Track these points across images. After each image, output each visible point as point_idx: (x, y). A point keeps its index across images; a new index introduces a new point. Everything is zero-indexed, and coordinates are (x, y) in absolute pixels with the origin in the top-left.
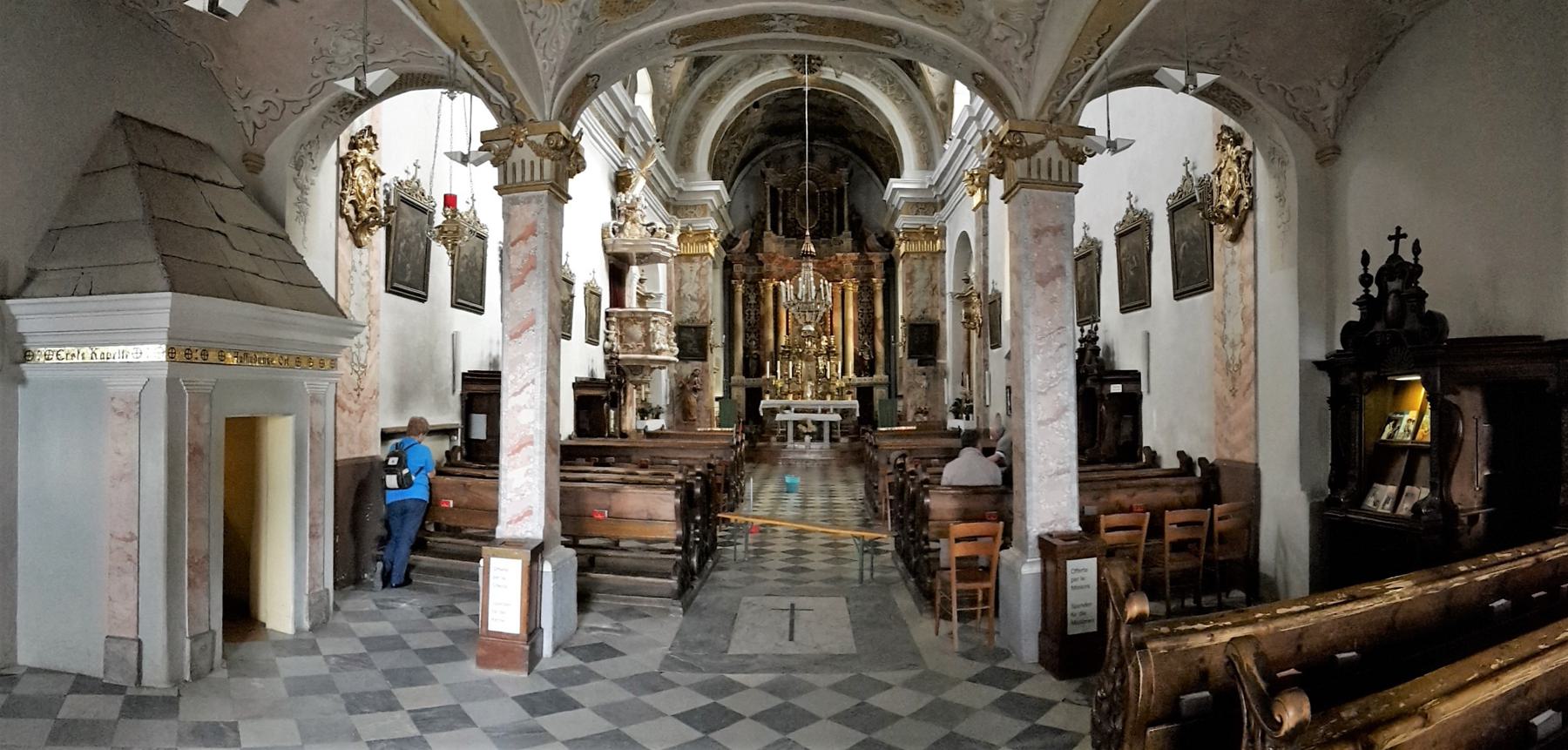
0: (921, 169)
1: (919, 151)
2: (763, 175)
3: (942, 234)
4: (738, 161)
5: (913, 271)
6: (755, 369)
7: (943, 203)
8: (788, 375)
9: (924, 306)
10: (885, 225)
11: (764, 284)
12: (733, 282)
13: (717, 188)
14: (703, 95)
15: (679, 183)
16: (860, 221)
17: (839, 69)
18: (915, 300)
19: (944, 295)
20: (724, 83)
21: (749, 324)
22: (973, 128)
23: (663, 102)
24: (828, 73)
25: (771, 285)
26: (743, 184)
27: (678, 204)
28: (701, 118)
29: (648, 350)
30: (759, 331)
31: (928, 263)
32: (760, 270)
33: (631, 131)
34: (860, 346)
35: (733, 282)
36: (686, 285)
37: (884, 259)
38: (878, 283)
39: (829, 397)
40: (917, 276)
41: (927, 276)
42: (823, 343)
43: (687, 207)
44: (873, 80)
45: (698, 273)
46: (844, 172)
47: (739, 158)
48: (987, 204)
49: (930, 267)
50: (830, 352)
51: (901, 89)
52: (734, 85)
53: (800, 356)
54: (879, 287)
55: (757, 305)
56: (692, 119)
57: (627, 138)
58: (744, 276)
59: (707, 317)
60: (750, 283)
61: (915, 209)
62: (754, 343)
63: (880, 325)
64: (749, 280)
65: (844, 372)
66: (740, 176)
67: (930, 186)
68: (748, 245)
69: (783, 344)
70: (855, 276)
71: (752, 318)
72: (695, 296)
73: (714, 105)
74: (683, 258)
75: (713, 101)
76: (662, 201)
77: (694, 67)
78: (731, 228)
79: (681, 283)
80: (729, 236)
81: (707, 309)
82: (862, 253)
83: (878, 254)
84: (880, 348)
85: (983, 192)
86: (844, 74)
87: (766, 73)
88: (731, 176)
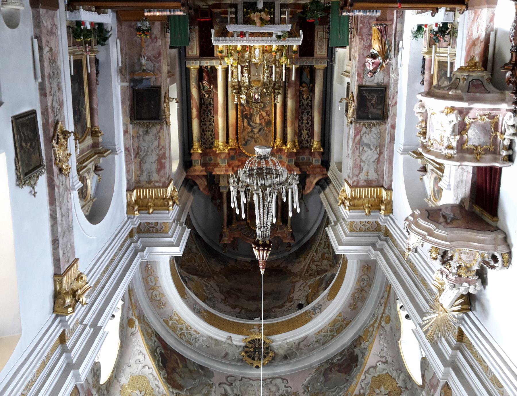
0: (155, 263)
1: (156, 278)
2: (292, 236)
3: (130, 206)
4: (314, 248)
5: (159, 171)
6: (305, 74)
7: (131, 234)
8: (276, 67)
9: (147, 138)
10: (192, 197)
11: (295, 146)
12: (322, 150)
13: (341, 248)
14: (347, 324)
15: (373, 254)
16: (213, 199)
17: (228, 344)
18: (156, 143)
19: (127, 149)
20: (329, 333)
21: (308, 113)
22: (75, 354)
23: (388, 328)
24: (238, 340)
25: (288, 146)
26: (309, 227)
27: (376, 233)
28: (350, 305)
29: (463, 113)
30: (300, 106)
31: (144, 178)
32: (297, 159)
33: (450, 351)
34: (212, 93)
35: (322, 150)
36: (372, 160)
37: (192, 169)
38: (196, 148)
39: (239, 48)
40: (155, 166)
41: (145, 166)
42: (244, 97)
43: (368, 230)
44: (198, 336)
45: (361, 170)
46: (226, 240)
47: (312, 254)
48: (55, 275)
49: (142, 174)
50: (239, 89)
51: (174, 329)
52: (321, 331)
53: (264, 84)
54: (196, 145)
55: (300, 129)
56: (359, 304)
57: (454, 342)
58: (311, 154)
59: (356, 129)
60: (307, 147)
61: (158, 227)
62: (305, 97)
63: (194, 112)
64: (307, 151)
65: (226, 71)
66: (311, 234)
67: (143, 250)
68: (308, 180)
69: (279, 96)
70: (216, 155)
71: (305, 118)
72: (365, 148)
73: (340, 315)
74: (374, 184)
75: (340, 318)
76: (394, 240)
77: (357, 356)
78: (322, 196)
79: (378, 161)
80: (323, 188)
81: (355, 136)
82: (211, 173)
83: (197, 173)
84: (194, 92)
85: (61, 287)
86: (224, 340)
87: (294, 339)
88: (319, 237)
